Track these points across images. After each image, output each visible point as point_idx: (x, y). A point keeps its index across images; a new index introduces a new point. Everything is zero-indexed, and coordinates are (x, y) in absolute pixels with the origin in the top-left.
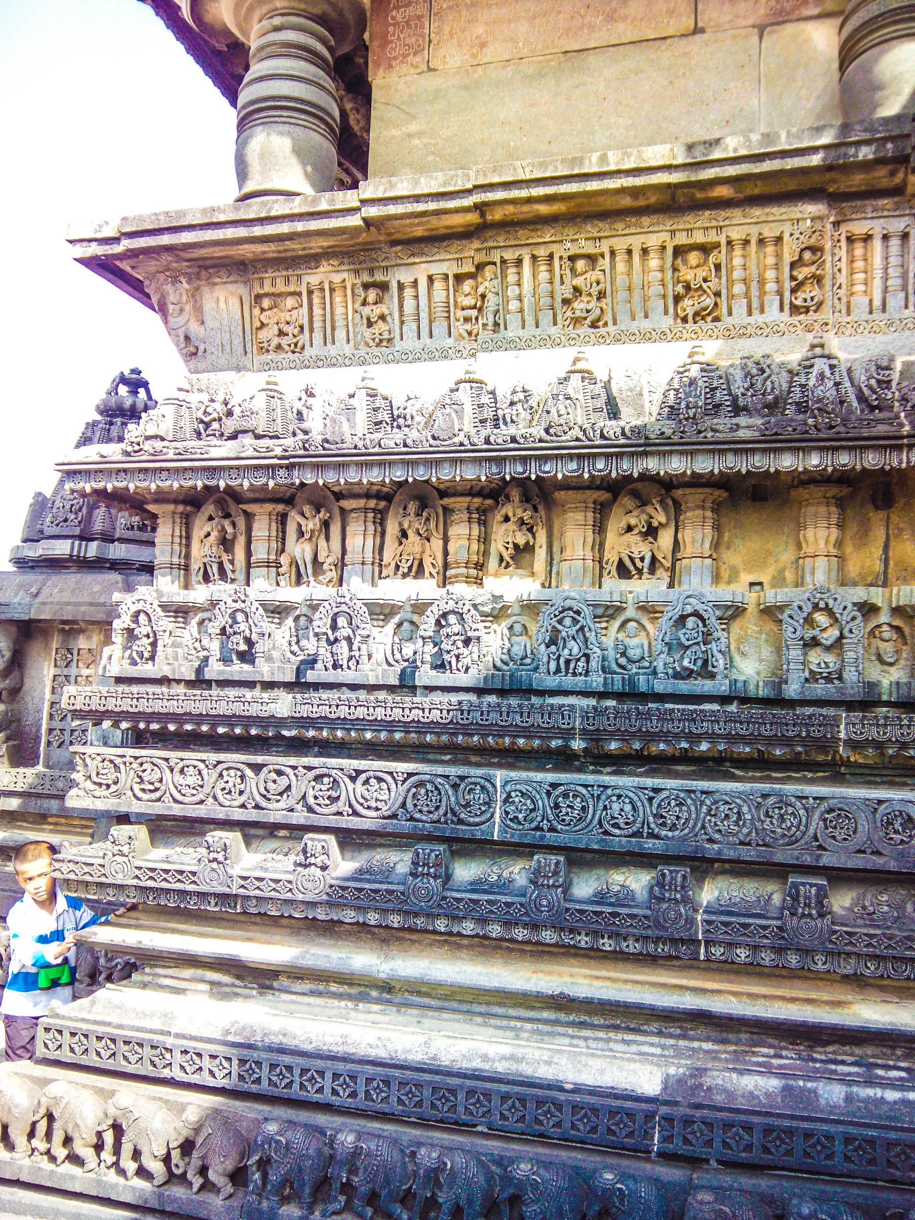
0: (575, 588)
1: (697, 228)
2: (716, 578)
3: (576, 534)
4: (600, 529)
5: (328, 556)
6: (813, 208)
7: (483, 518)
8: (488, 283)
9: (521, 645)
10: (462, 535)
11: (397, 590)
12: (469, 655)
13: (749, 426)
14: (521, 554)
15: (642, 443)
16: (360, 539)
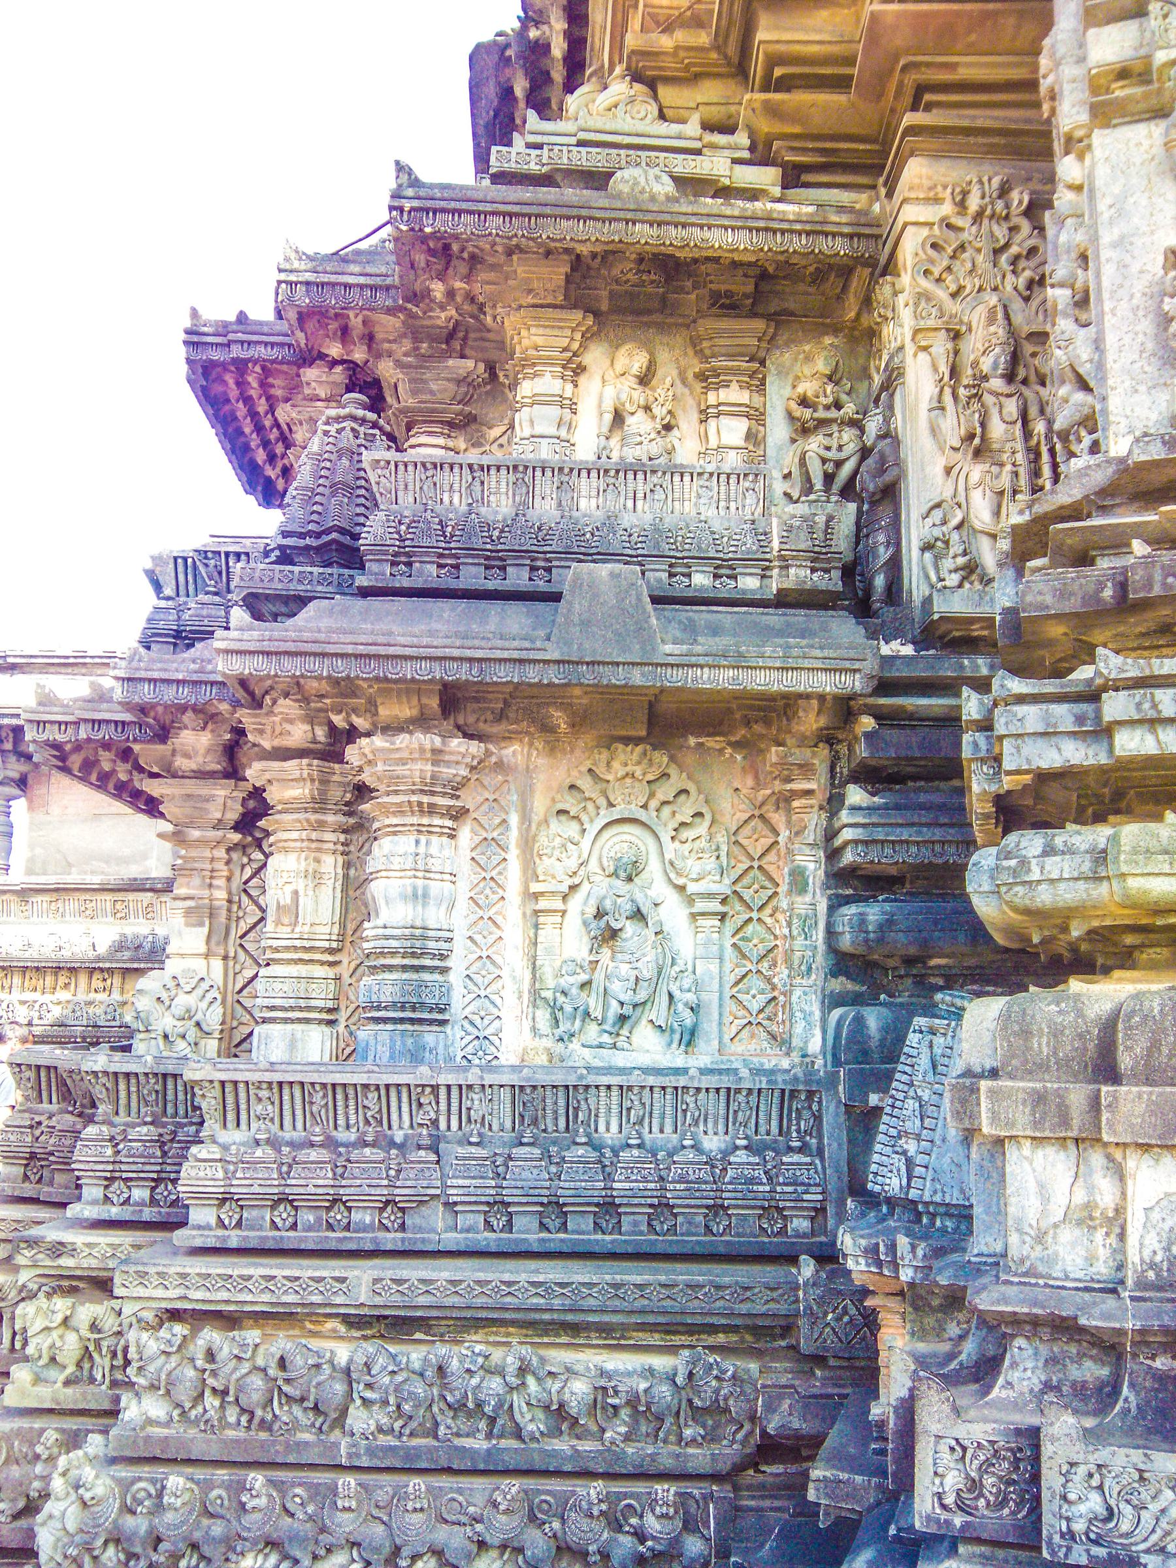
0: (82, 997)
1: (119, 896)
2: (122, 993)
3: (83, 979)
4: (91, 978)
5: (7, 985)
6: (150, 894)
7: (56, 974)
8: (60, 904)
9: (65, 1012)
10: (49, 979)
11: (29, 996)
12: (49, 1016)
13: (127, 954)
14: (67, 986)
15: (99, 959)
16: (17, 980)
